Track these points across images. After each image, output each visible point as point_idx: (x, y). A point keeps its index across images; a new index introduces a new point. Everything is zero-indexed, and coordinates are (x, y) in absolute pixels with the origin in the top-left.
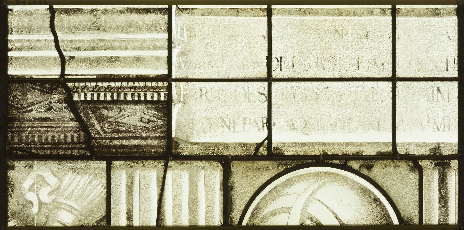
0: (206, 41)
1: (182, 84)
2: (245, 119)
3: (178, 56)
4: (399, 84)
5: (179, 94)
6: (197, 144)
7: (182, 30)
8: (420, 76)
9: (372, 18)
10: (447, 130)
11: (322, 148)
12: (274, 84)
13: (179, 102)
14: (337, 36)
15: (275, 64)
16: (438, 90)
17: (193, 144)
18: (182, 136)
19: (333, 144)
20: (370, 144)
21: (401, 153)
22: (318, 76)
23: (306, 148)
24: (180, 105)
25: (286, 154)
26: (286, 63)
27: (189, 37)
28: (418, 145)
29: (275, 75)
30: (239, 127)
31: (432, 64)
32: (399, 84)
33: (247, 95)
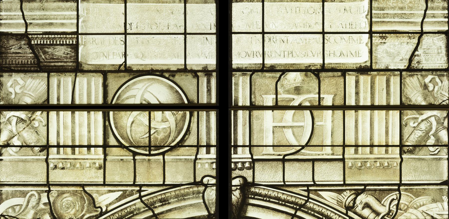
0: (95, 15)
1: (84, 36)
2: (114, 53)
3: (82, 23)
4: (187, 36)
5: (82, 41)
6: (91, 65)
7: (84, 10)
8: (198, 32)
9: (175, 4)
10: (211, 58)
11: (151, 67)
12: (128, 36)
13: (82, 45)
14: (158, 13)
15: (128, 26)
16: (207, 39)
17: (89, 65)
18: (84, 61)
19: (156, 65)
20: (174, 65)
21: (189, 69)
22: (149, 32)
23: (143, 67)
24: (83, 46)
25: (134, 70)
26: (134, 26)
27: (87, 13)
28: (197, 65)
29: (128, 31)
30: (111, 57)
31: (203, 27)
32: (187, 36)
33: (115, 42)
